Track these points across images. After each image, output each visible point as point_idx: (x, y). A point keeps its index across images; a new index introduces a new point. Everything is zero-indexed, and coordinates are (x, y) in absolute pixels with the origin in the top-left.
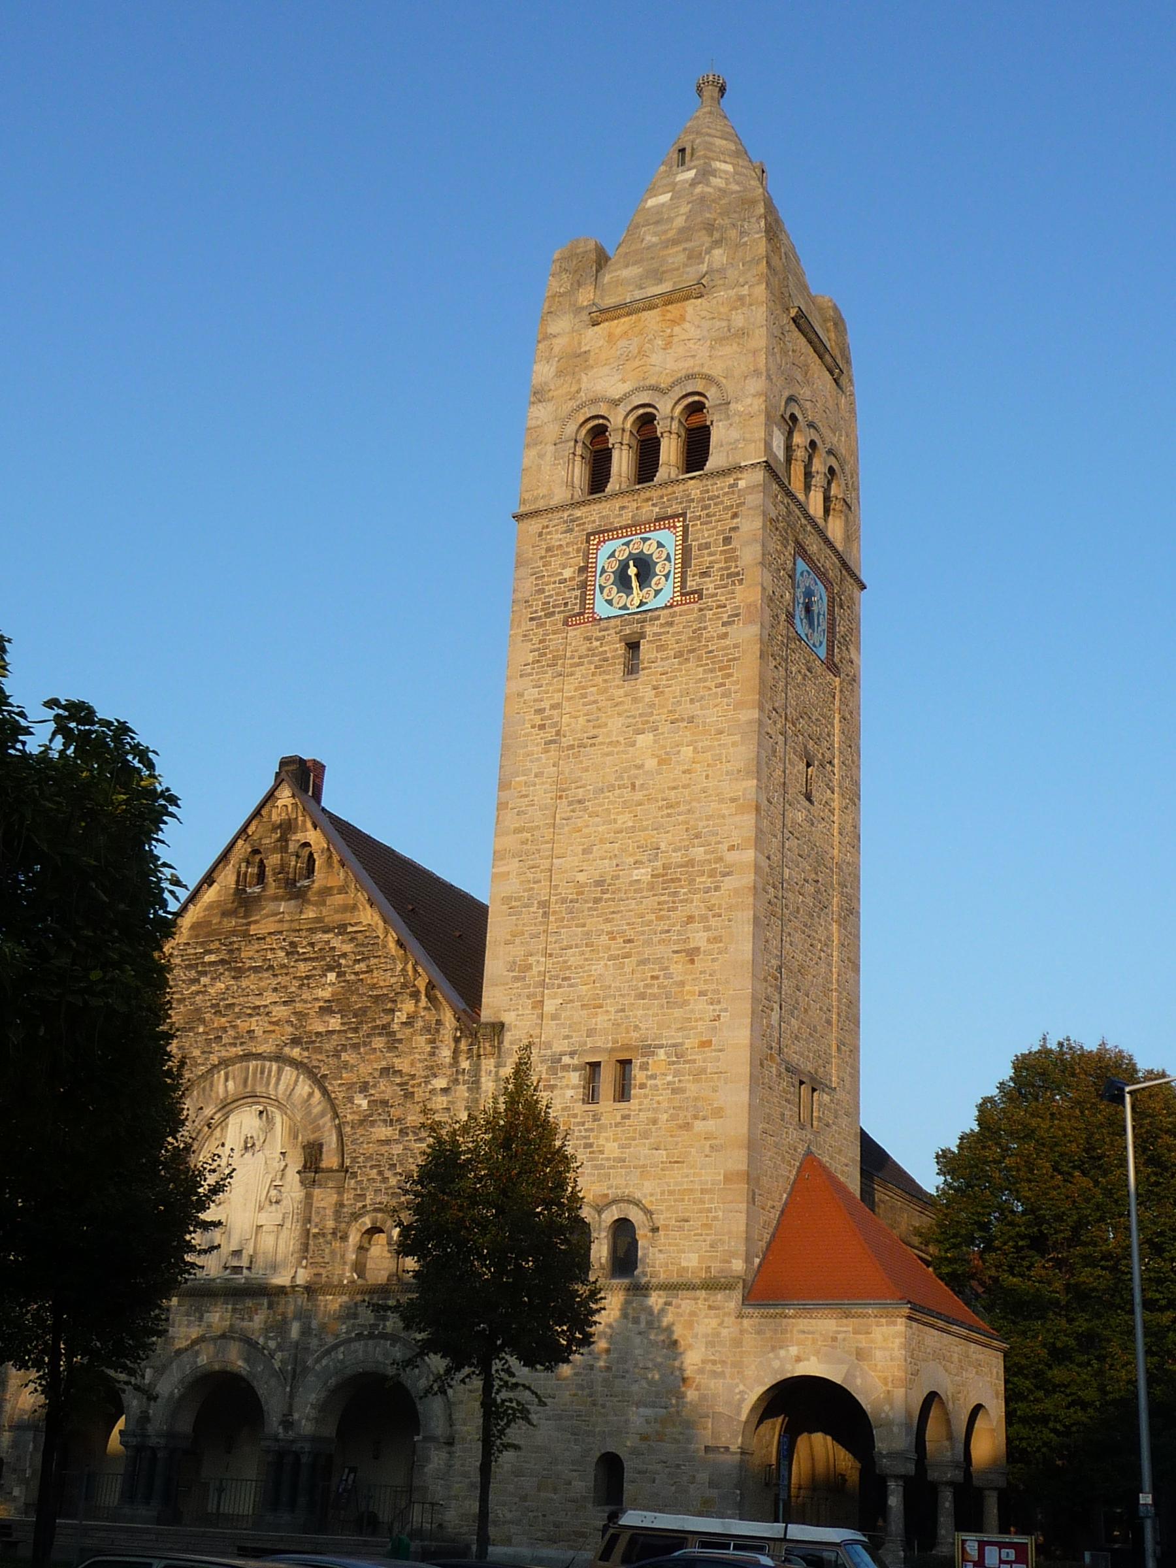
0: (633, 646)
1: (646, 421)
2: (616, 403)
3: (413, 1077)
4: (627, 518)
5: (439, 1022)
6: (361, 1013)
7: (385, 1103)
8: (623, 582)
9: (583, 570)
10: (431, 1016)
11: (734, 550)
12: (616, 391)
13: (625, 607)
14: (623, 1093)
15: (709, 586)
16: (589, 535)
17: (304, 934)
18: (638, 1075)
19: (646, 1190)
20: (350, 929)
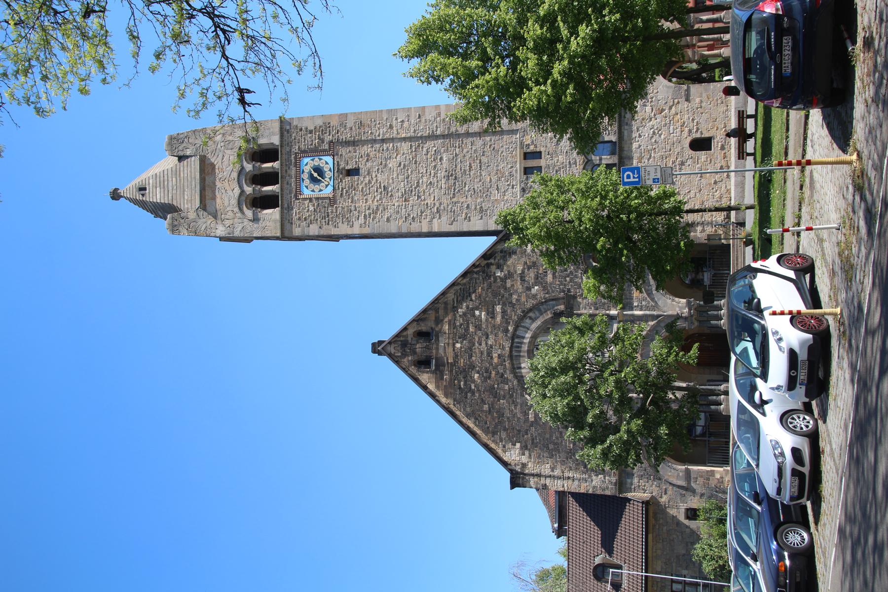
3: (526, 263)
5: (501, 251)
6: (495, 294)
7: (537, 277)
10: (498, 256)
11: (315, 128)
13: (330, 179)
15: (328, 138)
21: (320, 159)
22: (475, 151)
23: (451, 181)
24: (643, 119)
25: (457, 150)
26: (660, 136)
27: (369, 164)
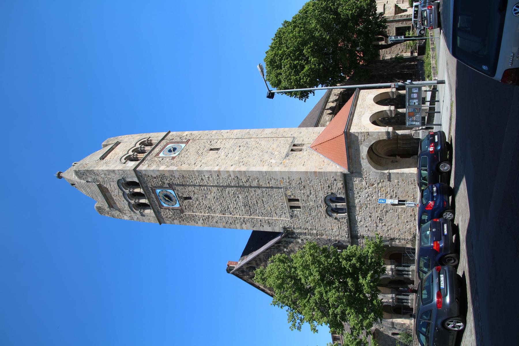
0: (186, 198)
2: (129, 203)
9: (169, 210)
12: (127, 203)
14: (298, 200)
18: (292, 197)
19: (322, 195)
22: (258, 195)
23: (248, 208)
24: (361, 188)
25: (247, 194)
26: (372, 197)
27: (196, 196)
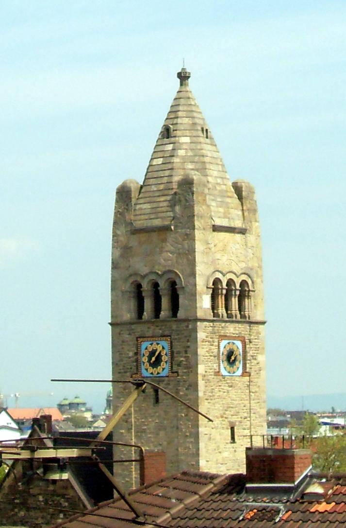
1: (156, 285)
4: (150, 333)
8: (152, 353)
13: (152, 373)
16: (137, 338)
17: (49, 495)
20: (66, 497)
21: (166, 362)
